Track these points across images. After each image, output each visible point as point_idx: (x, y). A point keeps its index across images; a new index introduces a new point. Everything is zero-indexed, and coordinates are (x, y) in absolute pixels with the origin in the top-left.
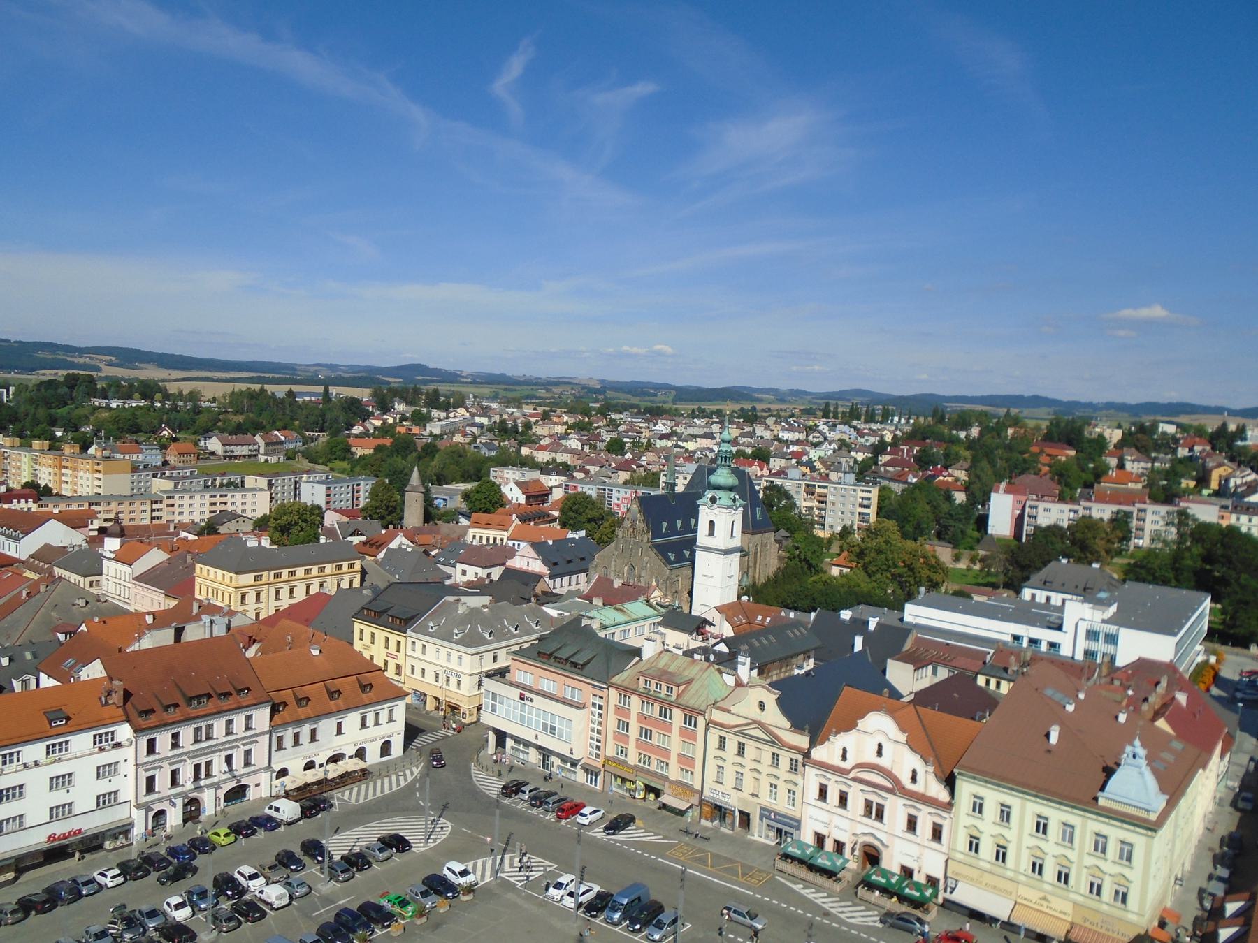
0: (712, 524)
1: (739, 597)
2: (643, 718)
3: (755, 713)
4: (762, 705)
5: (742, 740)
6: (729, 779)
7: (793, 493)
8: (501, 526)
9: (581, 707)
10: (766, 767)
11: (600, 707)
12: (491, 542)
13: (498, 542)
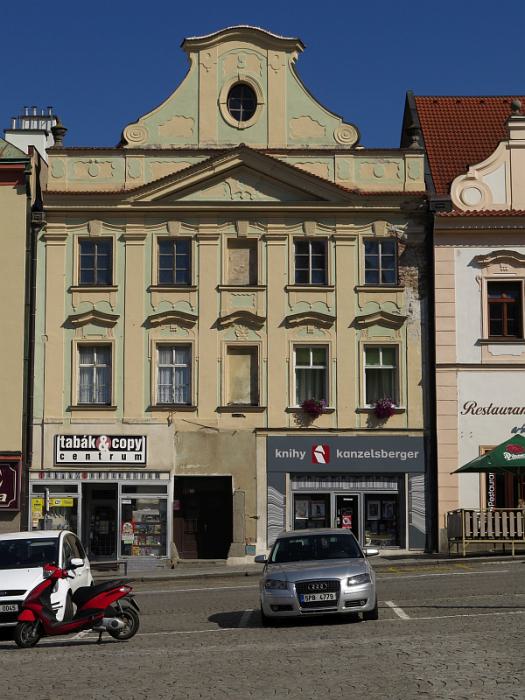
3: (218, 130)
4: (243, 99)
10: (278, 298)
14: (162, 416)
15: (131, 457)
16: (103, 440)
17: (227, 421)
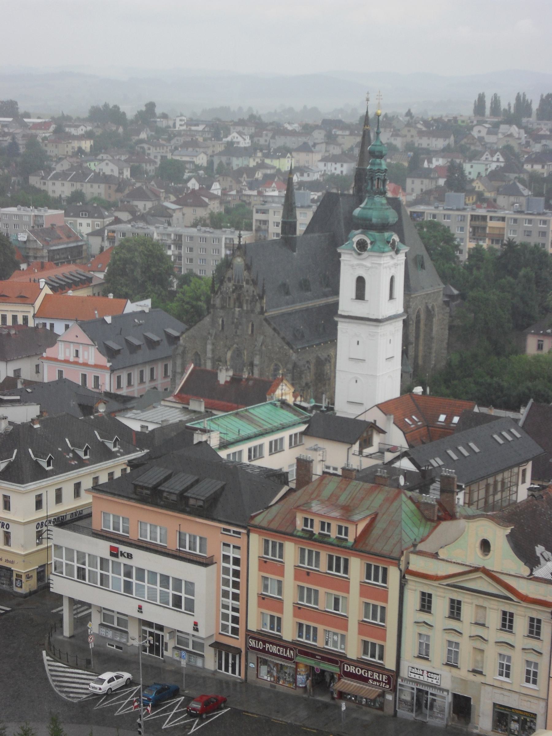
0: (360, 282)
1: (406, 390)
2: (299, 573)
3: (476, 558)
4: (485, 545)
5: (456, 596)
6: (438, 653)
7: (456, 231)
8: (25, 299)
9: (205, 563)
10: (493, 632)
11: (237, 561)
12: (9, 322)
13: (20, 321)
14: (447, 668)
15: (435, 682)
16: (425, 672)
17: (471, 677)
